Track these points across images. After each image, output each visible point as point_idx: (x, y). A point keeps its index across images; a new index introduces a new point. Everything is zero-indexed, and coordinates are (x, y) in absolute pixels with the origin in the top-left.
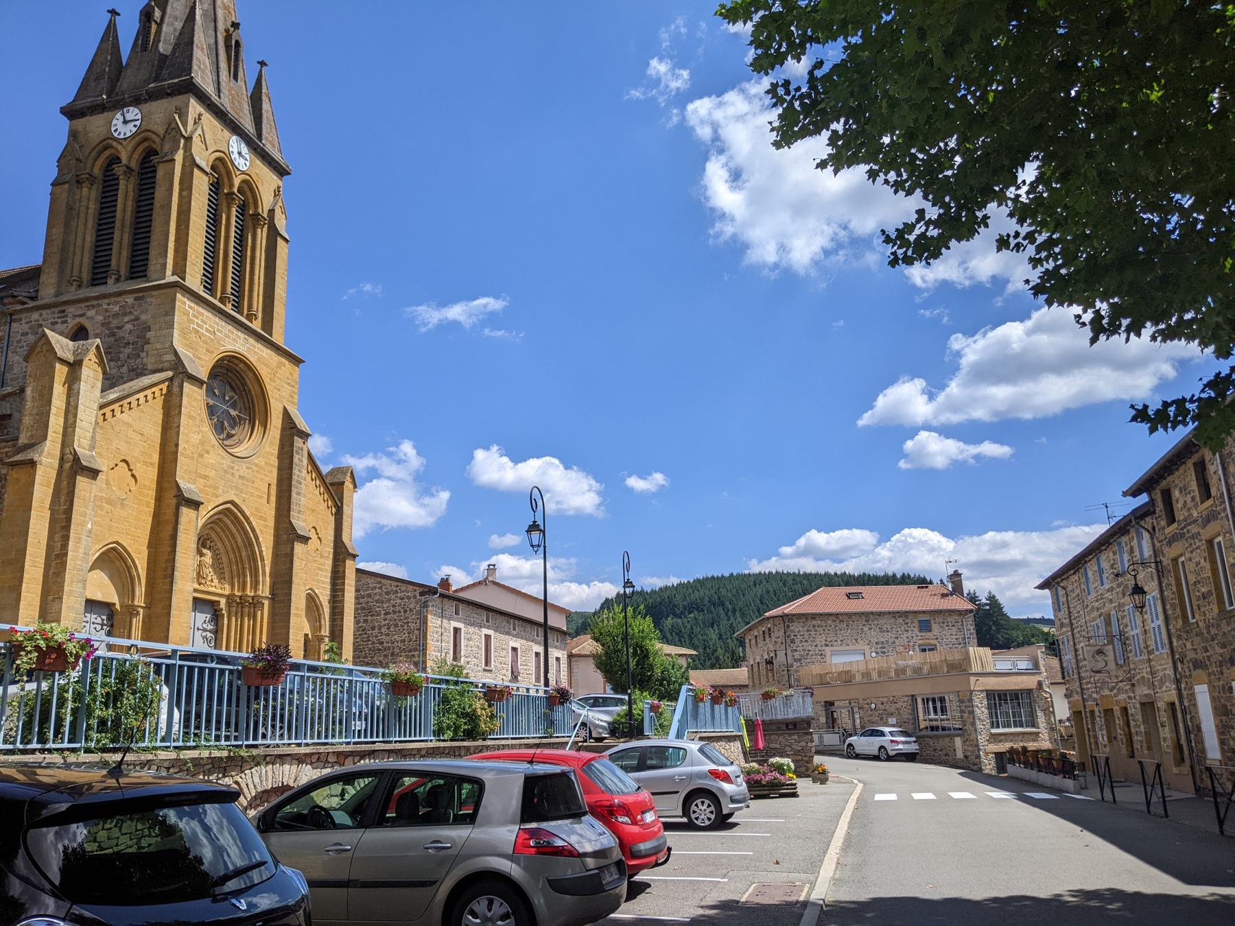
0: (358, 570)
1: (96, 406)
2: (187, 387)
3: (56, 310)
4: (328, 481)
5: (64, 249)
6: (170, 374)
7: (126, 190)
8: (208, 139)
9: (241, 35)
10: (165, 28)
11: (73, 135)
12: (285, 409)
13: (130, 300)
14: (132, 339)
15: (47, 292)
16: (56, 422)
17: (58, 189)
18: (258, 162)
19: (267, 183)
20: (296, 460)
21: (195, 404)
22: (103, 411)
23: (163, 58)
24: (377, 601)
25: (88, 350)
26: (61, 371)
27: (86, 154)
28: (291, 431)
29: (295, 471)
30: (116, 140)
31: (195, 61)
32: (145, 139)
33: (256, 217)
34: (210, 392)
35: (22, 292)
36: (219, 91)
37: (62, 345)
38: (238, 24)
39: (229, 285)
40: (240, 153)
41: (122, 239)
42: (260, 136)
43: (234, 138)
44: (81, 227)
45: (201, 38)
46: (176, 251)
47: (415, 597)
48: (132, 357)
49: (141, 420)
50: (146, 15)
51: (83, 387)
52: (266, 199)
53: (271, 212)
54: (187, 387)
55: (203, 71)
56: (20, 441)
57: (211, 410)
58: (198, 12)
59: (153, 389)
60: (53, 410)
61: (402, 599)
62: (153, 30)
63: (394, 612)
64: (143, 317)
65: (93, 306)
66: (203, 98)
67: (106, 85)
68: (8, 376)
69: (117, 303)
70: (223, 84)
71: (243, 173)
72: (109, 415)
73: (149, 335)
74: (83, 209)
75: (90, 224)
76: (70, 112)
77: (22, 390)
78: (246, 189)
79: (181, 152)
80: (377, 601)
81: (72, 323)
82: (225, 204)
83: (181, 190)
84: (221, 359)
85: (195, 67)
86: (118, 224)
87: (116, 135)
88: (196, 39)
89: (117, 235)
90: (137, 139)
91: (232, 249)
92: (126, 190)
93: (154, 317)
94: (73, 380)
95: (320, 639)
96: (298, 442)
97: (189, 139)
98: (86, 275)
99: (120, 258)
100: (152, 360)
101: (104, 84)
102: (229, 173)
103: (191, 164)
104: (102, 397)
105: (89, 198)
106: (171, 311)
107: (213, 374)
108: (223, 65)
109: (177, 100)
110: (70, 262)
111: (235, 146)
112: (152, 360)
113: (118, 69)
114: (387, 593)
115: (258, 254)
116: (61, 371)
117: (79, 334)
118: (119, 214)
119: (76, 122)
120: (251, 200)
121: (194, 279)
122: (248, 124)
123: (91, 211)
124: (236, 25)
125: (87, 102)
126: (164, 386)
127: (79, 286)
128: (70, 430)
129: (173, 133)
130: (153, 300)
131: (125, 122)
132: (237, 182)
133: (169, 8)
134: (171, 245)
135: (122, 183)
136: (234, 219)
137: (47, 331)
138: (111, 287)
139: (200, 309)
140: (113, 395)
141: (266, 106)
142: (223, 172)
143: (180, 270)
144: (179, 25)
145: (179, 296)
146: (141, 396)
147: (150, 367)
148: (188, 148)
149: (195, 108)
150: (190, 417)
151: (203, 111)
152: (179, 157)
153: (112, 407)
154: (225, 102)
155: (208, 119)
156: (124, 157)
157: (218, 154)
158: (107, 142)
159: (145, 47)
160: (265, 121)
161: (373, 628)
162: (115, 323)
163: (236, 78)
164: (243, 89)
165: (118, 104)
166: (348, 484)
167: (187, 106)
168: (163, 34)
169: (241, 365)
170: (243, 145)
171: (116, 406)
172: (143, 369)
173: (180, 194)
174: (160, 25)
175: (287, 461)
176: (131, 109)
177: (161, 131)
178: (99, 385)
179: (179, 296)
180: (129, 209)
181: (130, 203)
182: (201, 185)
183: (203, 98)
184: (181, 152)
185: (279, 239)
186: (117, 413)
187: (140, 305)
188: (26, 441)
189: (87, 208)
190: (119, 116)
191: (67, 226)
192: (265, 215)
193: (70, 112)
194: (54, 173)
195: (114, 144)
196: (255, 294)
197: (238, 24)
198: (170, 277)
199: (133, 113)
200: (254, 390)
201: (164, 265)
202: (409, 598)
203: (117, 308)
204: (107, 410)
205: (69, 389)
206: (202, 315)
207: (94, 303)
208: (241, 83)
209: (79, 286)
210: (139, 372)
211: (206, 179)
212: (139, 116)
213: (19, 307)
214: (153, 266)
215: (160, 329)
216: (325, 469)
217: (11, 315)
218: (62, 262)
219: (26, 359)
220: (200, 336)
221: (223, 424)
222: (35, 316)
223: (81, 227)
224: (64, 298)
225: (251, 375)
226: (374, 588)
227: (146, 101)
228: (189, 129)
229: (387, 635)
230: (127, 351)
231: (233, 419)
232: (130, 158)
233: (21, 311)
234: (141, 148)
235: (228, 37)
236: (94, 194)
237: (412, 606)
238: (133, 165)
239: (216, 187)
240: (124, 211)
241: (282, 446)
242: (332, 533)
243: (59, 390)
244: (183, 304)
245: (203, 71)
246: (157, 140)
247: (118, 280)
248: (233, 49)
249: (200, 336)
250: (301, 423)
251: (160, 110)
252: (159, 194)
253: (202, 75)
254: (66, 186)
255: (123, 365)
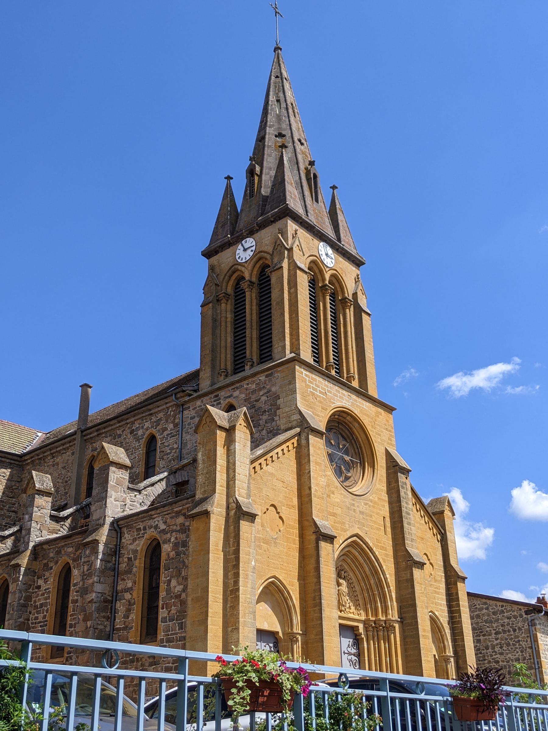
0: (469, 594)
1: (248, 462)
2: (312, 439)
3: (212, 396)
4: (429, 510)
5: (213, 351)
6: (298, 430)
7: (251, 298)
8: (304, 248)
9: (317, 169)
10: (264, 177)
11: (212, 268)
12: (386, 449)
13: (262, 378)
14: (267, 408)
15: (205, 384)
16: (221, 478)
17: (206, 308)
18: (341, 259)
19: (349, 274)
20: (402, 494)
21: (319, 452)
22: (253, 465)
23: (265, 199)
24: (486, 622)
25: (238, 417)
26: (221, 436)
27: (221, 280)
28: (394, 469)
29: (403, 504)
30: (240, 264)
31: (287, 193)
32: (260, 259)
33: (344, 300)
34: (328, 443)
35: (188, 388)
36: (307, 212)
37: (219, 415)
38: (314, 162)
39: (332, 357)
40: (327, 255)
41: (252, 334)
42: (339, 240)
43: (322, 244)
44: (223, 333)
45: (290, 177)
46: (291, 334)
47: (521, 616)
48: (269, 422)
49: (282, 468)
50: (251, 172)
51: (238, 446)
52: (350, 286)
53: (355, 295)
54: (312, 439)
55: (294, 199)
56: (197, 497)
57: (331, 457)
58: (285, 159)
59: (288, 444)
60: (218, 468)
61: (509, 618)
62: (256, 181)
63: (504, 632)
64: (273, 389)
65: (237, 388)
66: (296, 218)
67: (231, 227)
68: (184, 451)
69: (254, 382)
70: (309, 207)
71: (331, 269)
72: (258, 468)
73: (279, 402)
74: (223, 319)
75: (229, 329)
76: (208, 254)
77: (195, 460)
78: (334, 281)
79: (286, 260)
80: (486, 622)
81: (224, 403)
82: (321, 294)
83: (290, 288)
84: (333, 415)
85: (288, 197)
86: (248, 325)
87: (239, 261)
88: (286, 177)
89: (248, 331)
90: (254, 260)
91: (330, 329)
92: (251, 298)
93: (281, 387)
94: (230, 441)
95: (446, 660)
96: (401, 478)
97: (290, 250)
98: (230, 367)
99: (252, 349)
100: (283, 421)
101: (228, 227)
102: (321, 271)
103: (294, 267)
104: (252, 454)
105: (226, 310)
106: (292, 380)
107: (329, 428)
108: (307, 193)
109: (279, 224)
110: (218, 359)
111: (323, 249)
112: (283, 421)
113: (236, 216)
114: (494, 613)
115: (349, 329)
116: (221, 436)
117: (230, 408)
118: (248, 318)
119: (212, 259)
120: (339, 289)
121: (306, 354)
122: (330, 232)
123: (229, 320)
124: (312, 163)
125: (218, 243)
126: (295, 440)
127: (226, 376)
128: (231, 483)
129: (279, 248)
130: (278, 375)
131: (245, 250)
132: (327, 276)
133: (265, 163)
134: (287, 331)
135: (248, 294)
136: (328, 305)
137: (208, 406)
138: (248, 371)
139: (314, 376)
140: (259, 452)
141: (340, 217)
142: (317, 271)
143: (295, 348)
144: (273, 173)
145: (297, 367)
146: (279, 450)
147: (282, 427)
148: (290, 257)
149: (292, 226)
150: (317, 463)
151: (297, 228)
152: (285, 264)
153: (259, 461)
154: (312, 219)
155: (302, 233)
156: (247, 275)
157: (312, 258)
158: (235, 268)
159: (252, 195)
160: (341, 228)
161: (487, 648)
162: (254, 397)
163: (317, 201)
164: (323, 208)
165: (238, 239)
166: (447, 513)
167: (286, 226)
168: (263, 182)
169: (349, 418)
170: (328, 248)
171: (262, 460)
172: (278, 430)
173: (289, 292)
174: (260, 176)
175: (395, 495)
176: (248, 239)
177: (270, 249)
178: (249, 444)
179: (297, 367)
180: (254, 312)
181: (254, 307)
182: (303, 281)
183: (296, 218)
184: (286, 260)
185: (363, 314)
186: (264, 466)
187: (270, 380)
188: (201, 496)
189: (226, 318)
190: (240, 247)
191: (214, 334)
192: (351, 298)
193: (208, 254)
194: (201, 298)
195: (239, 267)
196: (351, 360)
197: (314, 162)
198: (289, 355)
199: (250, 242)
200: (361, 438)
201: (284, 347)
202: (515, 617)
203: (254, 386)
204: (256, 464)
205: (228, 450)
206: (315, 380)
207: (238, 385)
208: (321, 204)
209: (226, 376)
210: (274, 433)
211: (305, 276)
212: (254, 243)
213: (187, 398)
214: (276, 349)
215: (287, 395)
216: (426, 501)
217: (183, 405)
218: (213, 360)
219: (196, 432)
220: (316, 397)
221: (341, 468)
222: (199, 403)
223: (223, 333)
224: (216, 386)
225: (357, 425)
226: (482, 609)
227: (257, 231)
228: (290, 243)
229: (501, 654)
230: (265, 417)
231: (348, 463)
232: (251, 275)
233: (189, 401)
234: (258, 266)
235: (308, 172)
236: (229, 307)
237: (520, 624)
238: (254, 279)
239: (313, 283)
240: (251, 314)
241: (389, 483)
242: (441, 558)
243: (221, 452)
244: (301, 373)
245: (294, 199)
246: (268, 257)
247: (252, 366)
248: (312, 180)
249: (316, 397)
250: (402, 462)
251: (267, 235)
252: (274, 295)
253: (293, 201)
254: (210, 305)
255: (264, 429)
